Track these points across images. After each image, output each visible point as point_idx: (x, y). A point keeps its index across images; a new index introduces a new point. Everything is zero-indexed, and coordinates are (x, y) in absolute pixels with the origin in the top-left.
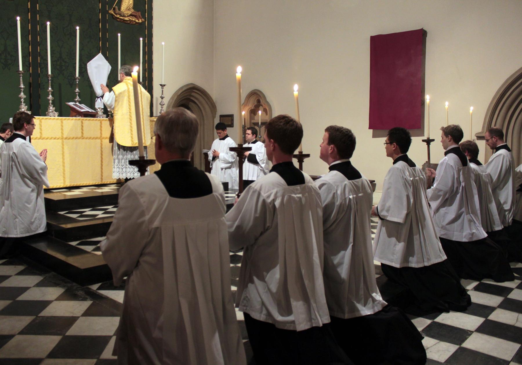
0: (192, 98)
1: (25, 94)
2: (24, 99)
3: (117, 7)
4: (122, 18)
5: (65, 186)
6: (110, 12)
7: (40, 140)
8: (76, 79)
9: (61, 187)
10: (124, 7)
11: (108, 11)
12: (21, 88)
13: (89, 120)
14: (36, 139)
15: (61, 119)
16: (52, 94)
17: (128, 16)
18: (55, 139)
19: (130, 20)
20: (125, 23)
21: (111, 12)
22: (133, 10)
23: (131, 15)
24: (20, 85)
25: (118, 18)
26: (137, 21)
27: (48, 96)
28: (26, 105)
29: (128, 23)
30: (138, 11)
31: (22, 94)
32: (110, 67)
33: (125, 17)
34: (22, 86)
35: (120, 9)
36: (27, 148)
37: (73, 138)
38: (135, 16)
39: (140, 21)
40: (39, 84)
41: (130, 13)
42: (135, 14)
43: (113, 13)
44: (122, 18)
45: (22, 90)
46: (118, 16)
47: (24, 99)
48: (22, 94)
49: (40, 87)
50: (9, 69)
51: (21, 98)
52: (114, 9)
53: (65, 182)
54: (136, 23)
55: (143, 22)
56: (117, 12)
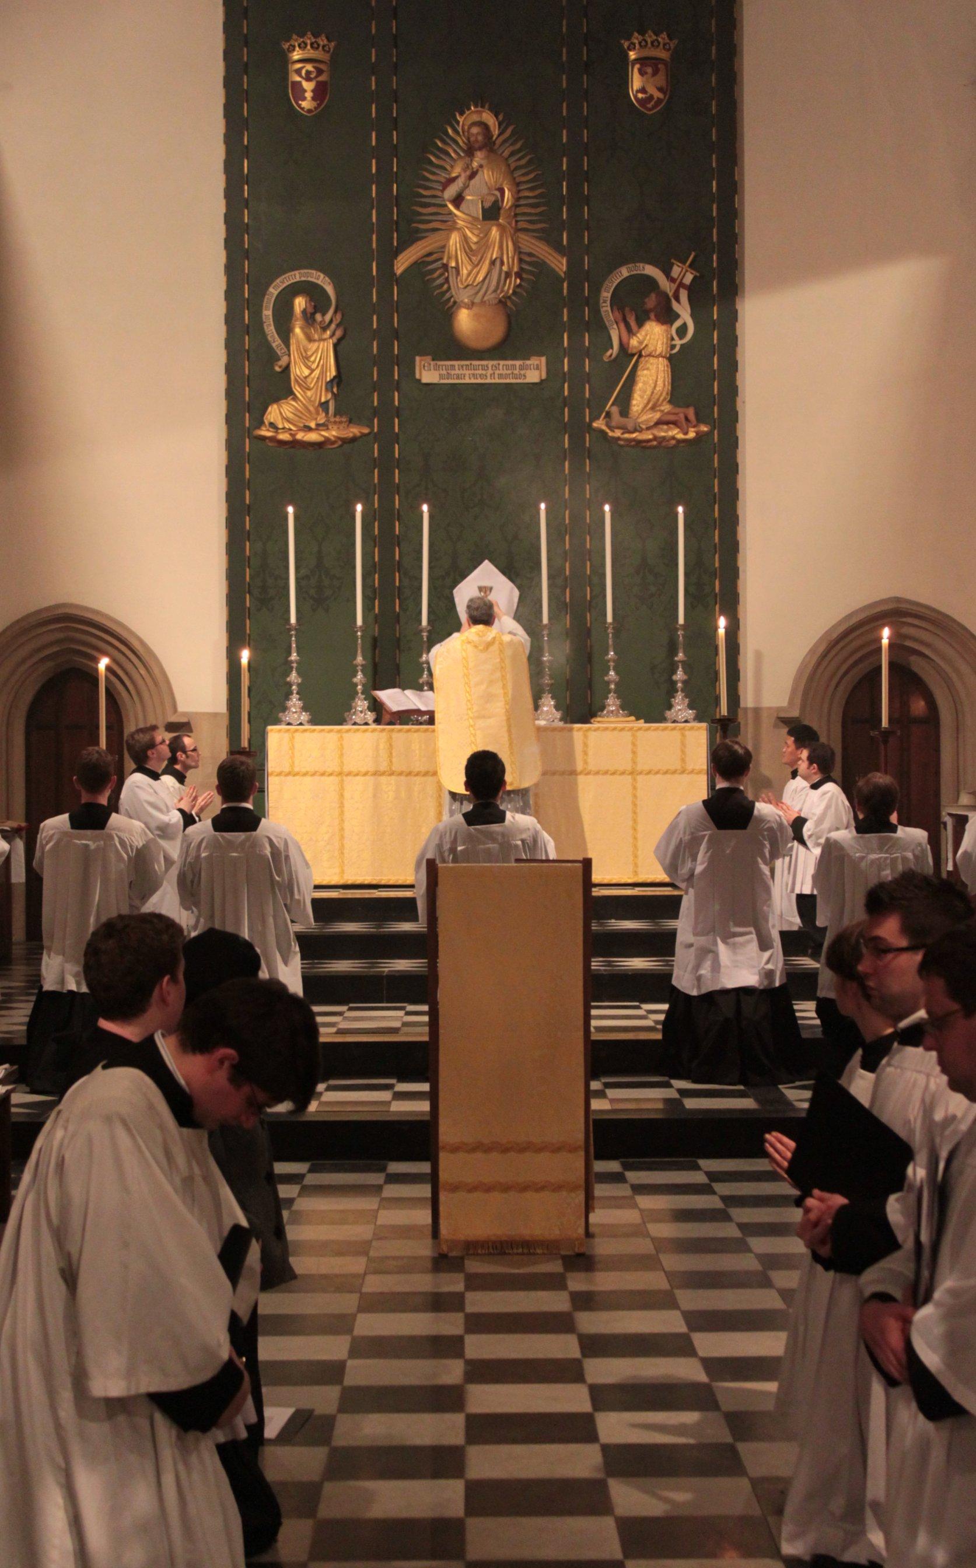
0: (908, 643)
1: (299, 674)
2: (299, 685)
3: (615, 410)
4: (626, 436)
5: (341, 882)
6: (595, 425)
7: (290, 778)
8: (421, 631)
9: (333, 883)
10: (638, 402)
11: (590, 425)
12: (292, 662)
13: (409, 731)
14: (279, 774)
15: (339, 731)
16: (362, 671)
17: (648, 429)
18: (323, 774)
19: (655, 438)
20: (643, 447)
21: (599, 424)
22: (667, 407)
23: (659, 423)
24: (290, 654)
25: (619, 439)
26: (680, 436)
27: (355, 676)
28: (300, 699)
29: (655, 447)
30: (688, 406)
31: (294, 674)
32: (516, 593)
33: (641, 431)
34: (294, 656)
35: (625, 412)
36: (137, 790)
37: (314, 774)
38: (675, 423)
39: (692, 435)
40: (398, 640)
41: (657, 416)
42: (672, 418)
43: (604, 428)
44: (626, 436)
45: (295, 665)
46: (618, 433)
47: (299, 685)
48: (294, 674)
49: (398, 647)
50: (327, 610)
51: (290, 685)
52: (608, 415)
53: (343, 872)
54: (679, 441)
55: (700, 435)
56: (613, 424)
